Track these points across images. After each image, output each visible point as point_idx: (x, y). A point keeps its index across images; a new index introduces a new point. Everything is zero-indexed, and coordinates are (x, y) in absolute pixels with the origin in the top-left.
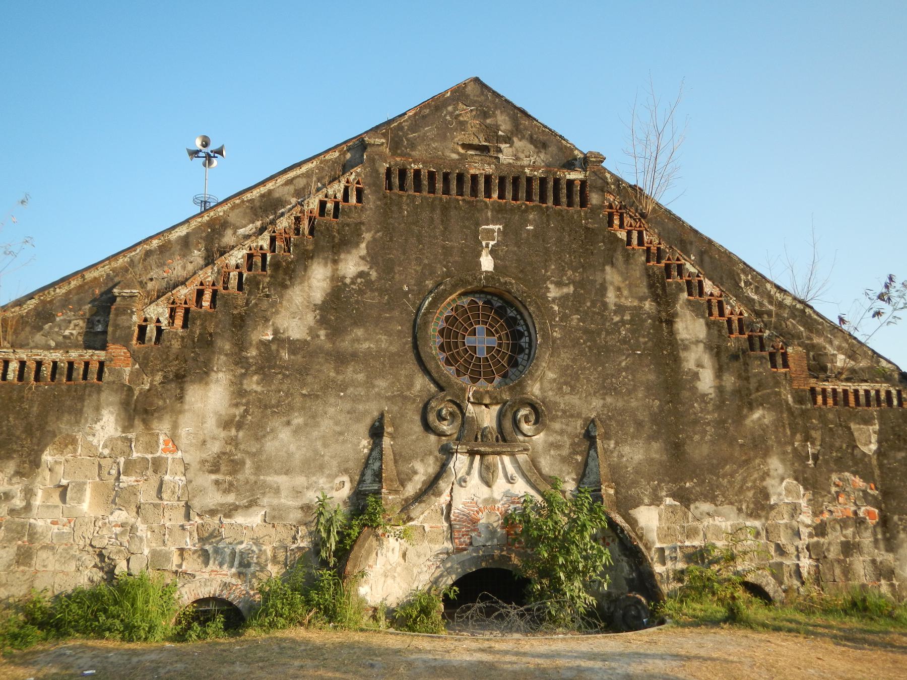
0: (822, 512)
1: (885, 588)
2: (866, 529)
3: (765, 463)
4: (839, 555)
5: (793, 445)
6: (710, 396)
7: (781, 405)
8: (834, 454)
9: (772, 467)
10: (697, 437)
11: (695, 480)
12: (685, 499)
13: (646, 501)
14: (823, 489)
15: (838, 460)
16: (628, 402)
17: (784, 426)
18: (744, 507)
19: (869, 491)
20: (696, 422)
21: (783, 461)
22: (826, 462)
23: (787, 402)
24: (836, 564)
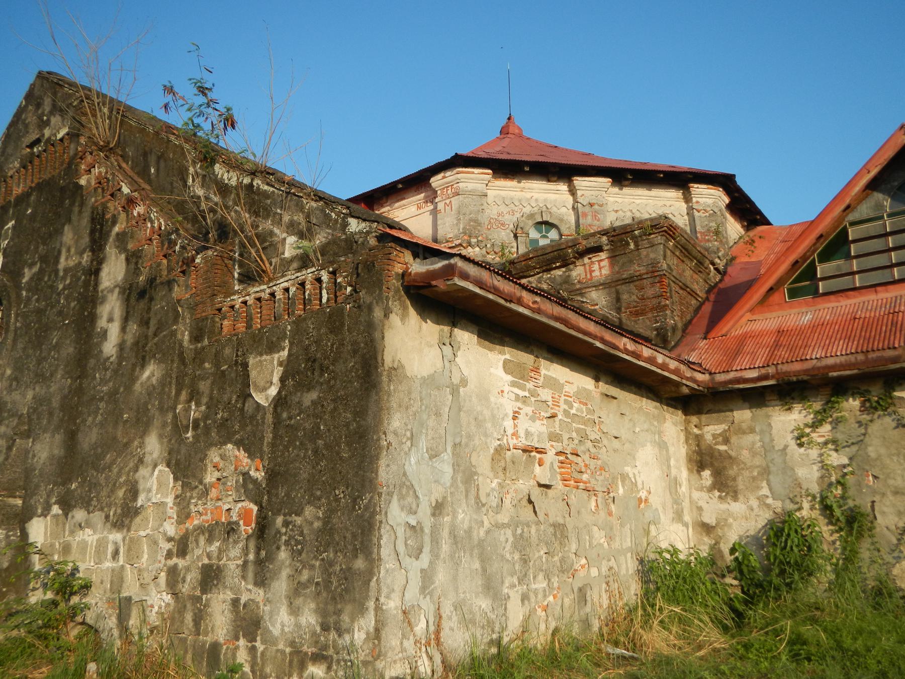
0: (188, 516)
1: (242, 656)
2: (236, 542)
3: (142, 445)
4: (194, 588)
5: (175, 409)
6: (112, 360)
7: (174, 348)
8: (219, 416)
9: (148, 448)
10: (90, 419)
11: (80, 480)
12: (67, 506)
13: (39, 511)
14: (194, 476)
15: (223, 425)
16: (49, 387)
17: (170, 383)
18: (111, 514)
19: (252, 473)
20: (93, 398)
21: (161, 436)
22: (207, 429)
23: (181, 346)
24: (189, 606)
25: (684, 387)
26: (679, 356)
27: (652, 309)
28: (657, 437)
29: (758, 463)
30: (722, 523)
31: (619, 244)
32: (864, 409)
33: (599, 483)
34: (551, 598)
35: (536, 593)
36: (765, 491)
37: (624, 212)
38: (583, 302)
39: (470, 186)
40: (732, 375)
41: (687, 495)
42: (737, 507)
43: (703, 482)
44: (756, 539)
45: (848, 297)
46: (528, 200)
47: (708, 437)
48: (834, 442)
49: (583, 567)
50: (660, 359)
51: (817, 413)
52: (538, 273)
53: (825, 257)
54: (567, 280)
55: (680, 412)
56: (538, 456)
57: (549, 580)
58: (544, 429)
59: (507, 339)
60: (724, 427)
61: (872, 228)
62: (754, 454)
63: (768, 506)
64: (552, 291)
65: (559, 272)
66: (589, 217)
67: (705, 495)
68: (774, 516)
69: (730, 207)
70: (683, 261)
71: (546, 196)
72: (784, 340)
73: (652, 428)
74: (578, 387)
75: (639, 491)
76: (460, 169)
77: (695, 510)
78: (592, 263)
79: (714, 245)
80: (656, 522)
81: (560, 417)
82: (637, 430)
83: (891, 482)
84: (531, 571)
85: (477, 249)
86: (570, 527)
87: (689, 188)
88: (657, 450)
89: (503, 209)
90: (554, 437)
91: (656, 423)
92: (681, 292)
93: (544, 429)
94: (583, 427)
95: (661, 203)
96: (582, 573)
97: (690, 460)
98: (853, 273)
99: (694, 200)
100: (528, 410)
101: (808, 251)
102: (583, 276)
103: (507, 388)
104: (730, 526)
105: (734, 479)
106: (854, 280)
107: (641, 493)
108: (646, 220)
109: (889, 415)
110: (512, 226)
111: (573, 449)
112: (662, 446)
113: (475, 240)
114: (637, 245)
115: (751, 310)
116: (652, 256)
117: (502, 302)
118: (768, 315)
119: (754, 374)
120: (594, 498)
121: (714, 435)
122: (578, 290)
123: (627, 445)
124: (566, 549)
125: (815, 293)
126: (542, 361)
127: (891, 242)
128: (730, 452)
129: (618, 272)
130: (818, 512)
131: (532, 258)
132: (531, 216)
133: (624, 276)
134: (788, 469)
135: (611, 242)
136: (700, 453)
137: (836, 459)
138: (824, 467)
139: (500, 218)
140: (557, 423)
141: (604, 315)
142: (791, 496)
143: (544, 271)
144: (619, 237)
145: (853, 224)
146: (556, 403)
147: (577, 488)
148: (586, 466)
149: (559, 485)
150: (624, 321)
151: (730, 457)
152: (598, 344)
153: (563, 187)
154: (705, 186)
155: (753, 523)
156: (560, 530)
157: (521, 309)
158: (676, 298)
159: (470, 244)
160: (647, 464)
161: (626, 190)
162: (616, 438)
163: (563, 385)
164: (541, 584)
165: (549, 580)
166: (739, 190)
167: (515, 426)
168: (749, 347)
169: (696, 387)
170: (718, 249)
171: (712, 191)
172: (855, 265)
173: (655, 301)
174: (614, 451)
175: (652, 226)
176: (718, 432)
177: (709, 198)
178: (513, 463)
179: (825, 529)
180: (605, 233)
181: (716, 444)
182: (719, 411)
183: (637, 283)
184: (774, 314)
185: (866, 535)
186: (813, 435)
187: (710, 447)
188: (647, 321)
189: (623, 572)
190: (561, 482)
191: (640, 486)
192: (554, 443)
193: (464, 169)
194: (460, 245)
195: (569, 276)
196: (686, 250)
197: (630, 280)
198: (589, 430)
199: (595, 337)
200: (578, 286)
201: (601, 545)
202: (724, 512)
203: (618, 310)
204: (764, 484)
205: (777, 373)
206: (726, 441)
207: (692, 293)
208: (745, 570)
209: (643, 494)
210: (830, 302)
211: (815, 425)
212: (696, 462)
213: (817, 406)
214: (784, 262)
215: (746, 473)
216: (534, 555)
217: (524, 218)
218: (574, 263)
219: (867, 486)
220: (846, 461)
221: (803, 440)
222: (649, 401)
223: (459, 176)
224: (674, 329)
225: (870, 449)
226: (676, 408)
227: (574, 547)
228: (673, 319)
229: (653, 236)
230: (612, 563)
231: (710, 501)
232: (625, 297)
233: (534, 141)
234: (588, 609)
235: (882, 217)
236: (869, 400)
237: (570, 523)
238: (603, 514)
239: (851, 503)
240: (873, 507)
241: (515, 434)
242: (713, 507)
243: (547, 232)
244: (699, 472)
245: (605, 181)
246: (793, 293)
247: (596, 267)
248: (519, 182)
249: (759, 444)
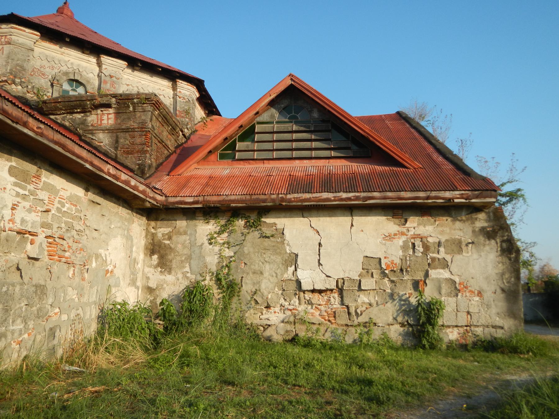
25: (148, 203)
26: (150, 183)
27: (138, 152)
28: (126, 232)
29: (186, 253)
30: (160, 287)
31: (123, 106)
32: (246, 226)
33: (77, 259)
34: (26, 336)
35: (13, 332)
36: (187, 269)
37: (133, 87)
38: (93, 139)
39: (21, 40)
40: (178, 199)
41: (141, 270)
42: (170, 278)
43: (152, 262)
44: (177, 296)
45: (249, 164)
46: (66, 62)
47: (160, 235)
48: (228, 243)
49: (56, 314)
50: (133, 182)
51: (222, 226)
52: (64, 114)
53: (243, 138)
54: (83, 122)
55: (144, 218)
56: (31, 237)
57: (26, 323)
58: (38, 219)
59: (15, 151)
60: (170, 229)
61: (268, 127)
62: (184, 247)
63: (187, 278)
64: (72, 128)
65: (79, 116)
66: (108, 85)
67: (152, 270)
68: (190, 283)
69: (199, 99)
70: (163, 126)
72: (211, 183)
73: (123, 226)
74: (71, 194)
75: (107, 266)
76: (14, 26)
77: (145, 279)
78: (103, 114)
79: (185, 120)
80: (117, 285)
81: (53, 212)
82: (113, 226)
83: (253, 267)
84: (11, 317)
85: (20, 87)
86: (49, 287)
87: (176, 82)
88: (124, 240)
89: (45, 63)
90: (44, 225)
91: (126, 224)
92: (159, 144)
93: (38, 219)
94: (71, 221)
95: (157, 87)
96: (54, 318)
97: (146, 248)
98: (254, 151)
99: (178, 90)
100: (27, 204)
101: (234, 133)
102: (95, 122)
103: (9, 187)
104: (164, 289)
105: (171, 261)
106: (254, 154)
107: (109, 267)
108: (143, 94)
109: (258, 230)
110: (50, 77)
111: (60, 235)
112: (129, 238)
113: (19, 81)
114: (134, 108)
115: (198, 163)
116: (143, 117)
117: (9, 122)
118: (206, 167)
119: (190, 200)
120: (72, 269)
121: (163, 234)
122: (90, 130)
123: (103, 236)
124: (44, 302)
125: (234, 159)
126: (44, 172)
127: (275, 137)
128: (171, 245)
129: (119, 124)
130: (214, 282)
131: (60, 102)
132: (66, 74)
133: (123, 127)
134: (201, 257)
135: (118, 103)
136: (153, 244)
137: (228, 253)
138: (221, 257)
139: (42, 69)
140: (50, 216)
141: (106, 150)
142: (201, 272)
143: (68, 113)
144: (123, 101)
145: (259, 123)
146: (51, 202)
147: (60, 261)
148: (69, 247)
149: (45, 258)
150: (119, 156)
151: (171, 248)
152: (88, 166)
153: (93, 60)
154: (186, 83)
155: (178, 288)
156: (41, 290)
157: (26, 131)
158: (154, 147)
159: (14, 82)
160: (116, 248)
161: (137, 73)
162: (96, 230)
163: (59, 190)
164: (19, 326)
165: (26, 323)
166: (206, 91)
167: (13, 214)
168: (192, 184)
169: (155, 204)
170: (187, 123)
171: (190, 87)
172: (256, 146)
173: (140, 147)
174: (93, 238)
175: (145, 99)
176: (166, 233)
177: (187, 91)
178: (7, 241)
179: (215, 291)
180: (115, 96)
181: (163, 240)
182: (169, 220)
183: (131, 133)
184: (210, 167)
185: (236, 295)
186: (218, 238)
187: (160, 241)
188: (134, 159)
189: (88, 316)
190: (47, 257)
191: (109, 262)
192: (45, 230)
193: (17, 27)
194: (6, 81)
195: (85, 120)
196: (166, 119)
197: (126, 130)
198: (75, 223)
199: (86, 161)
200: (91, 128)
201: (73, 300)
202: (162, 280)
203: (116, 148)
204: (187, 265)
205: (204, 201)
206: (170, 238)
207: (166, 147)
208: (167, 315)
209: (110, 268)
210: (240, 164)
211: (220, 233)
212: (150, 249)
213: (223, 222)
214: (219, 137)
215: (178, 258)
216: (16, 305)
217: (60, 74)
218: (91, 112)
219: (241, 268)
220: (232, 254)
221: (212, 241)
222: (124, 209)
223: (13, 30)
224: (150, 166)
225: (245, 248)
226: (142, 215)
227: (50, 301)
228: (150, 160)
229: (145, 105)
230: (80, 311)
231: (155, 274)
232: (122, 140)
233: (81, 24)
234: (56, 342)
235: (273, 123)
236: (249, 222)
237: (50, 285)
238: (77, 279)
239: (231, 278)
240: (242, 280)
241: (12, 220)
242: (155, 277)
243: (77, 87)
244: (151, 256)
245: (123, 64)
246: (222, 157)
247: (105, 117)
248: (61, 48)
249: (188, 241)
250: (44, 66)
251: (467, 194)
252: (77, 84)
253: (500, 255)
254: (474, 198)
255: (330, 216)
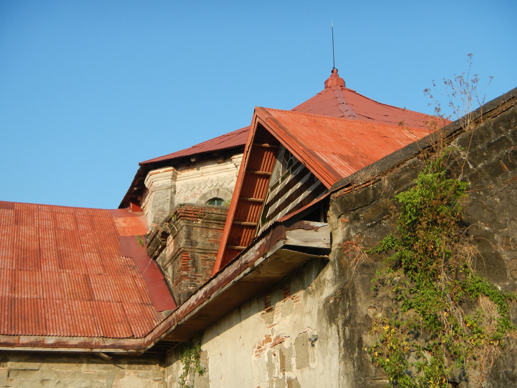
25: (102, 354)
46: (206, 182)
71: (218, 175)
89: (189, 194)
114: (177, 229)
132: (204, 196)
175: (176, 213)
223: (151, 177)
248: (198, 169)
250: (188, 197)
251: (263, 243)
252: (219, 201)
253: (345, 357)
254: (268, 251)
255: (230, 328)
